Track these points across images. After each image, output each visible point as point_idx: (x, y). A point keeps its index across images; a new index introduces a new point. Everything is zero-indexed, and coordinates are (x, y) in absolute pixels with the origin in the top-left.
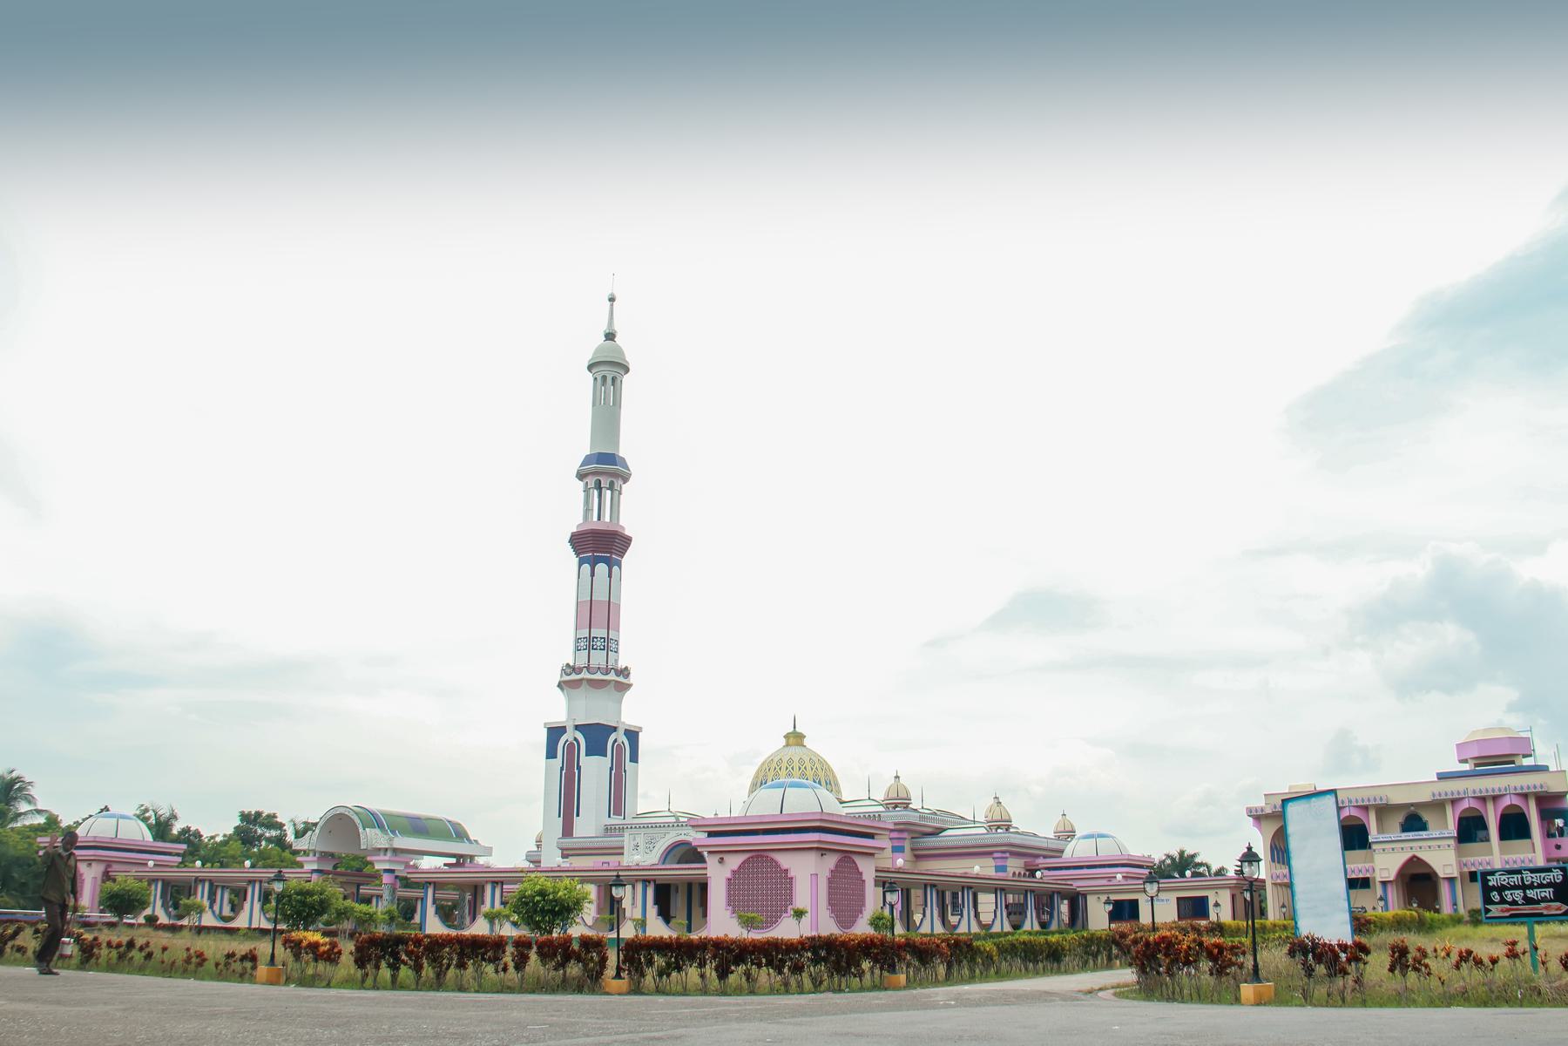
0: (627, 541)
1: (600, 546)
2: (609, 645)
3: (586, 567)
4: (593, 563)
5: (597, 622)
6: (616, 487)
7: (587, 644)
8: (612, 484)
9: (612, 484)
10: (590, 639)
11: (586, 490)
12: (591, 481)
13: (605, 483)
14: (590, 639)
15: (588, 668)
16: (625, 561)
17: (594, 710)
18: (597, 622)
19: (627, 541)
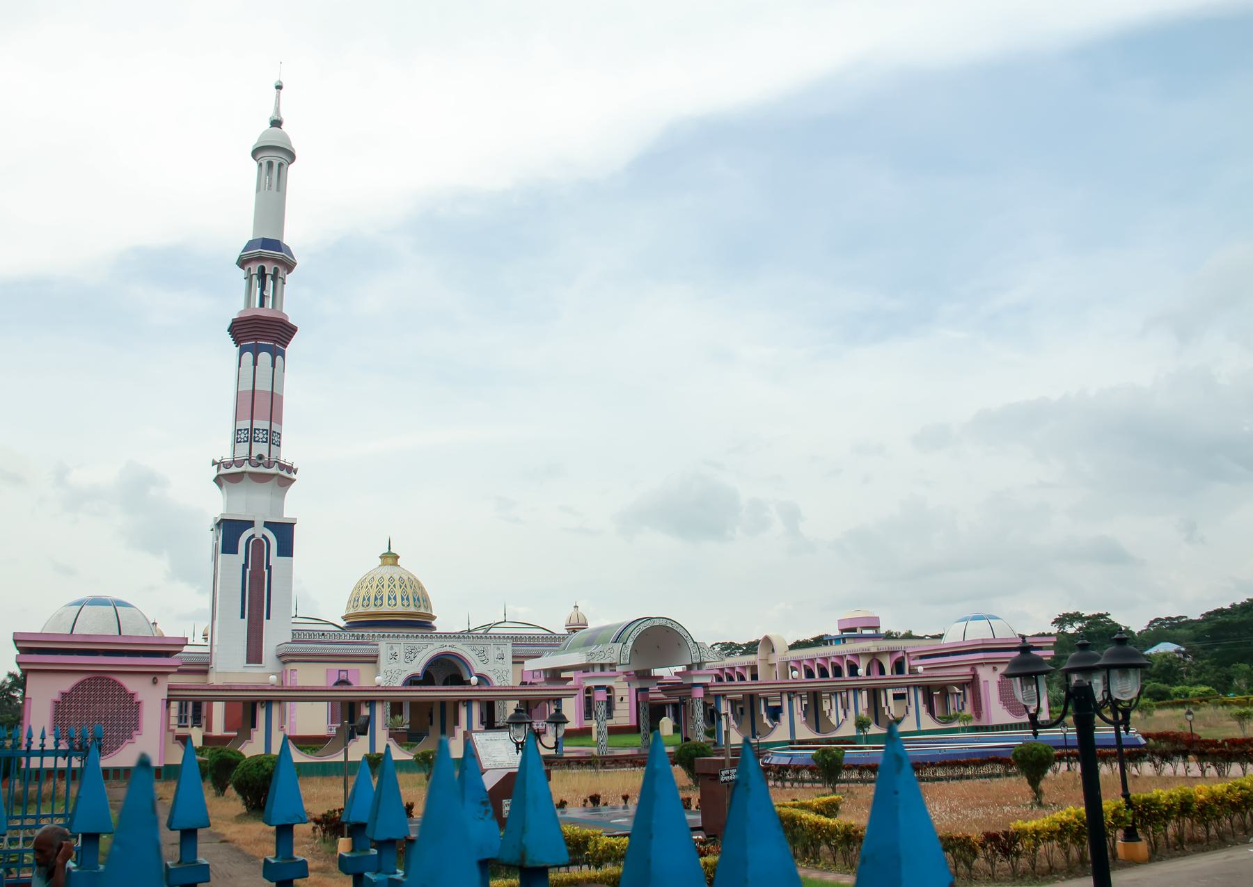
0: (292, 330)
1: (262, 334)
2: (273, 438)
3: (248, 356)
4: (256, 352)
5: (259, 414)
6: (280, 275)
7: (246, 436)
8: (276, 271)
9: (276, 271)
10: (252, 430)
11: (249, 278)
12: (255, 268)
13: (269, 270)
14: (252, 430)
15: (249, 460)
16: (288, 350)
17: (253, 505)
18: (259, 414)
19: (292, 330)
